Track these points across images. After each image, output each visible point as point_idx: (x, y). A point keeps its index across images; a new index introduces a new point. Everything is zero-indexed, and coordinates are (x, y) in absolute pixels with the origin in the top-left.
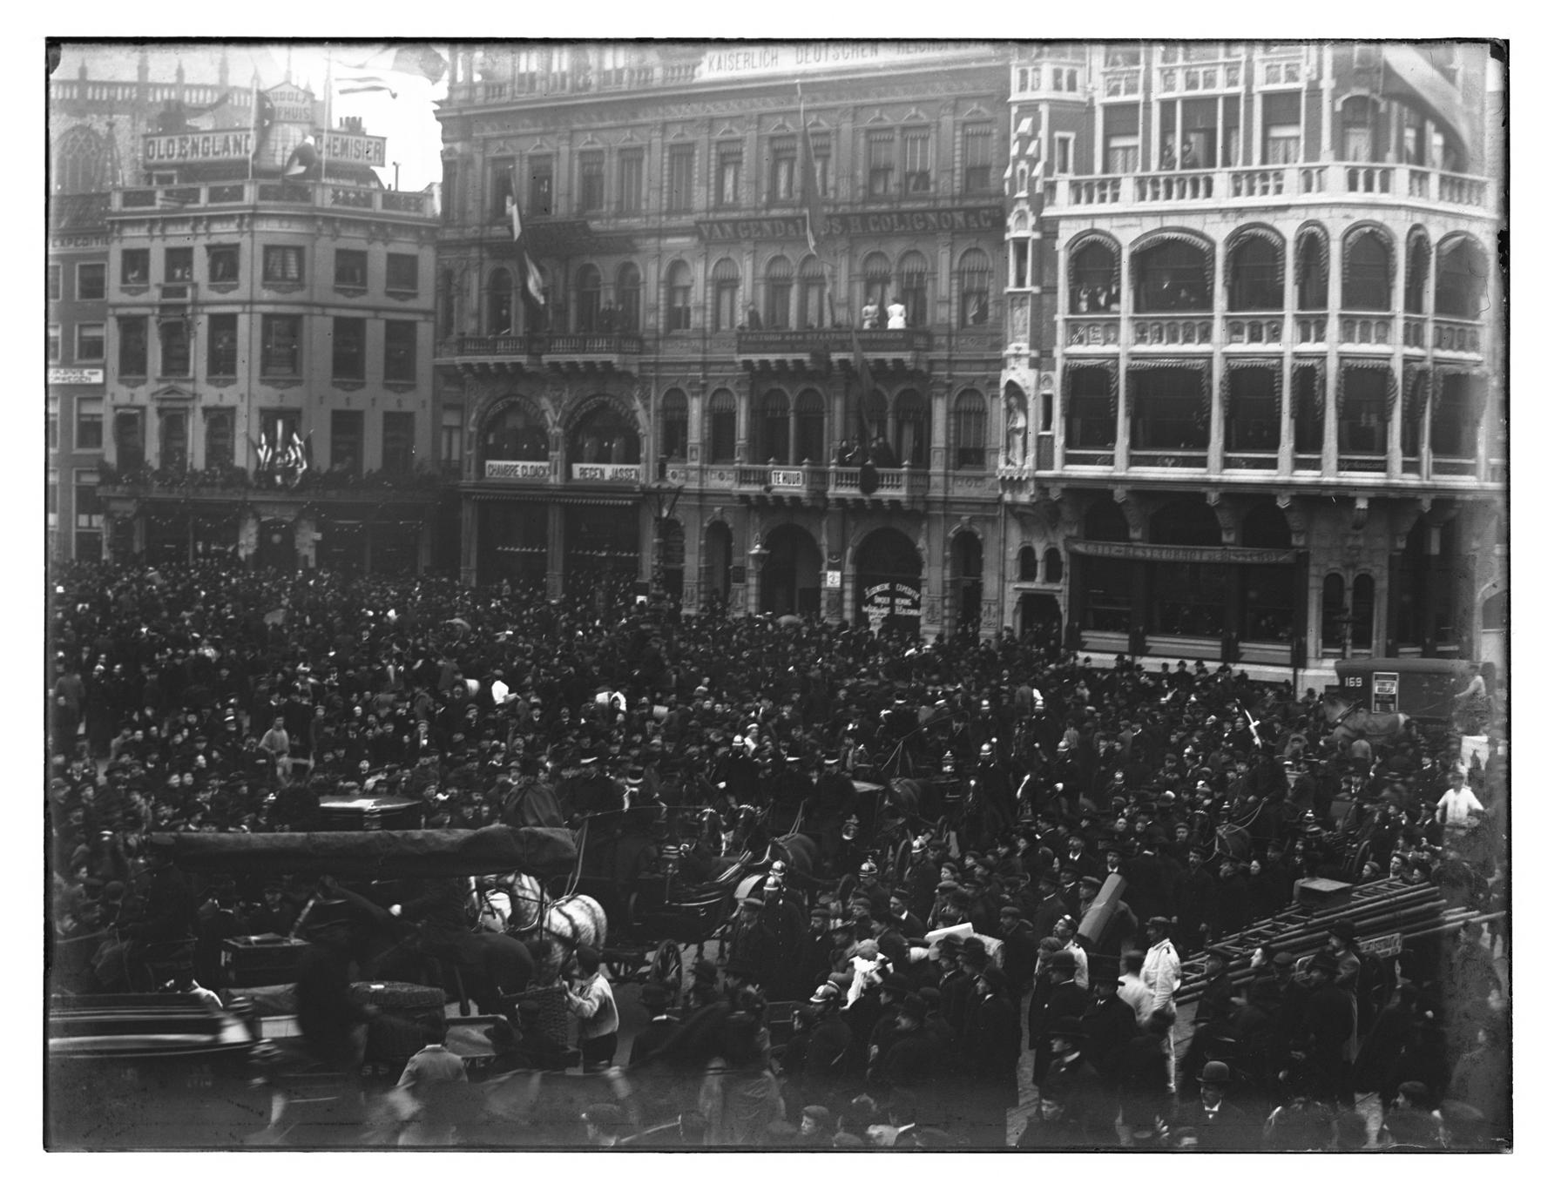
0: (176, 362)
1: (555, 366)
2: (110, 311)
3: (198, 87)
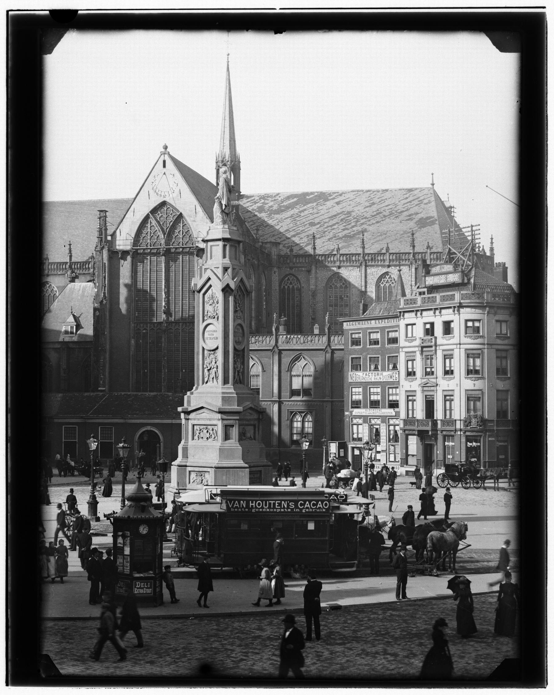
2: (401, 350)
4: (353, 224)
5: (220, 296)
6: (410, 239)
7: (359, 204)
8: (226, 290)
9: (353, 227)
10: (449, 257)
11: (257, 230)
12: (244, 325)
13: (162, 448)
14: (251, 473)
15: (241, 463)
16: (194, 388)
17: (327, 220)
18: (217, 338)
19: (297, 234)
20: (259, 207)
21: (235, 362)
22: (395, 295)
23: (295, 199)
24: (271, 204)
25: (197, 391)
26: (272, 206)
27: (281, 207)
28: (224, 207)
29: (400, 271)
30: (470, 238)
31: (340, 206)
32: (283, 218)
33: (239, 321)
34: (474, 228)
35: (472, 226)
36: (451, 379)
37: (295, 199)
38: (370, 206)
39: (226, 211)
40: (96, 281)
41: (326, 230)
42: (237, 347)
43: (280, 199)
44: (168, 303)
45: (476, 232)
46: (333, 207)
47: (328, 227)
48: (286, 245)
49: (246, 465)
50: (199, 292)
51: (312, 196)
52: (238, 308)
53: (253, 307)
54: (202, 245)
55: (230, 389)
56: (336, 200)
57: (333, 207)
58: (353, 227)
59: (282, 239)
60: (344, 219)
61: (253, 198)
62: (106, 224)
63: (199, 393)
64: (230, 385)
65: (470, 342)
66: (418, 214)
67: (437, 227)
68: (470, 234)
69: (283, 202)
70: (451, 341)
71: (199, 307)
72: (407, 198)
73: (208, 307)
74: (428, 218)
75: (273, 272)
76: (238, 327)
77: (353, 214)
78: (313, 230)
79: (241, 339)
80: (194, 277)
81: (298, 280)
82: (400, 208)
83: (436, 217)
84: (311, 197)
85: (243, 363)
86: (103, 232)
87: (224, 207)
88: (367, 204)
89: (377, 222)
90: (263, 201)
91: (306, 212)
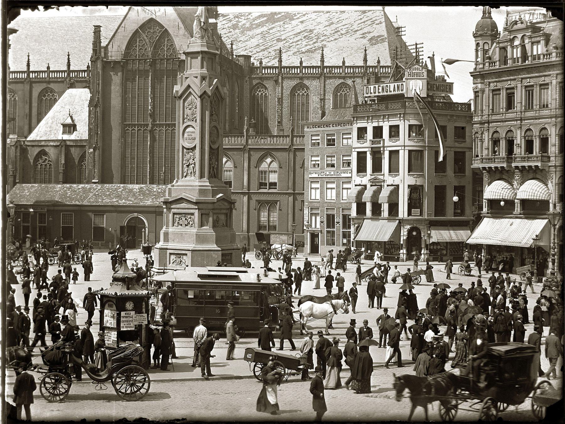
0: (377, 168)
1: (517, 167)
2: (353, 150)
3: (385, 67)
4: (315, 41)
5: (198, 102)
6: (362, 55)
7: (320, 23)
8: (203, 96)
9: (315, 43)
10: (397, 70)
11: (232, 44)
12: (218, 127)
13: (147, 232)
14: (223, 255)
15: (214, 247)
16: (175, 181)
17: (292, 37)
18: (195, 139)
19: (266, 49)
20: (233, 25)
21: (210, 159)
22: (349, 102)
23: (265, 18)
24: (244, 22)
25: (177, 184)
26: (244, 24)
27: (252, 25)
28: (202, 24)
29: (354, 82)
30: (414, 54)
31: (304, 25)
32: (254, 34)
33: (214, 123)
34: (418, 46)
35: (416, 44)
36: (396, 176)
37: (265, 18)
38: (329, 25)
39: (204, 27)
40: (91, 87)
41: (291, 45)
42: (212, 146)
43: (252, 18)
44: (153, 107)
45: (420, 50)
46: (297, 25)
47: (293, 42)
48: (257, 58)
49: (219, 249)
50: (180, 97)
51: (280, 15)
52: (214, 113)
53: (227, 111)
54: (183, 57)
55: (206, 183)
56: (301, 20)
57: (297, 25)
58: (315, 43)
59: (253, 53)
60: (307, 36)
61: (228, 17)
62: (100, 37)
63: (178, 186)
64: (205, 179)
65: (412, 144)
66: (370, 32)
67: (386, 44)
68: (414, 51)
69: (254, 21)
70: (398, 143)
71: (179, 110)
72: (361, 19)
73: (188, 112)
74: (378, 37)
75: (245, 81)
76: (214, 128)
77: (315, 31)
78: (280, 45)
79: (215, 139)
80: (176, 85)
81: (266, 88)
82: (355, 27)
83: (386, 36)
84: (278, 16)
85: (217, 160)
86: (98, 44)
87: (202, 24)
88: (327, 23)
89: (336, 39)
90: (237, 19)
91: (274, 30)
